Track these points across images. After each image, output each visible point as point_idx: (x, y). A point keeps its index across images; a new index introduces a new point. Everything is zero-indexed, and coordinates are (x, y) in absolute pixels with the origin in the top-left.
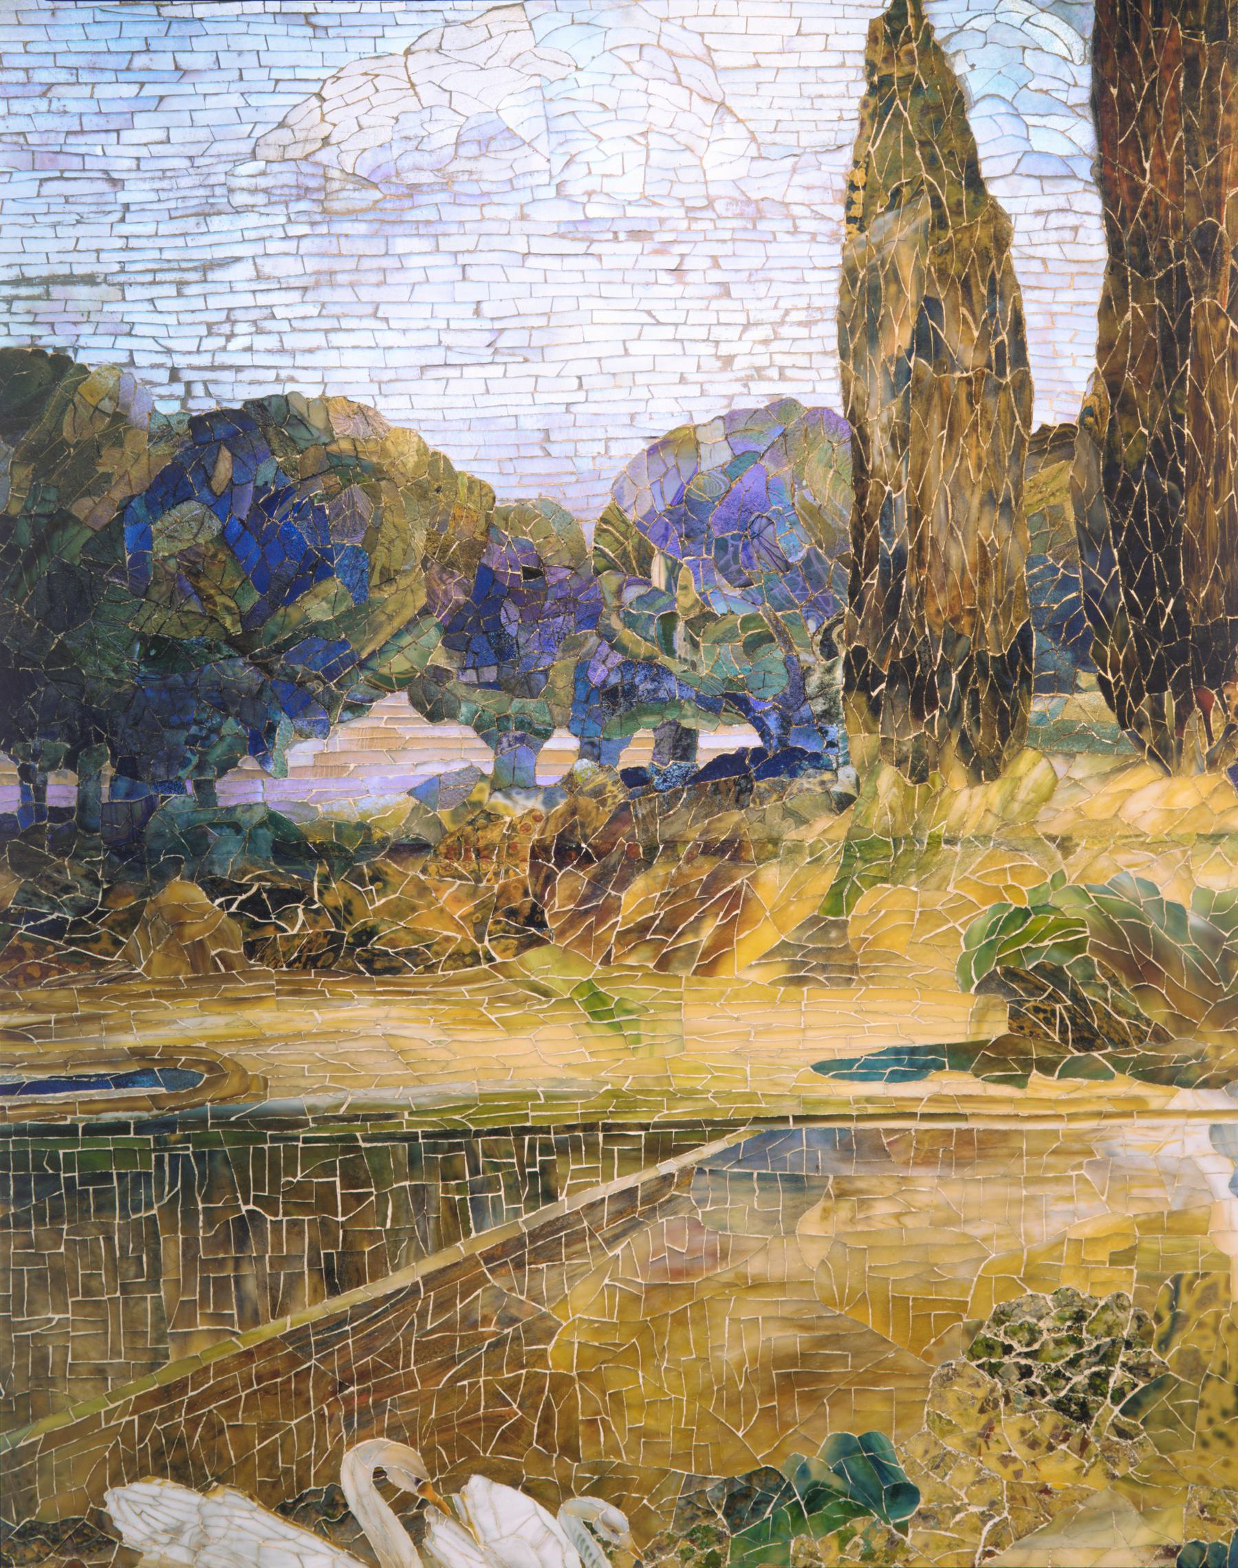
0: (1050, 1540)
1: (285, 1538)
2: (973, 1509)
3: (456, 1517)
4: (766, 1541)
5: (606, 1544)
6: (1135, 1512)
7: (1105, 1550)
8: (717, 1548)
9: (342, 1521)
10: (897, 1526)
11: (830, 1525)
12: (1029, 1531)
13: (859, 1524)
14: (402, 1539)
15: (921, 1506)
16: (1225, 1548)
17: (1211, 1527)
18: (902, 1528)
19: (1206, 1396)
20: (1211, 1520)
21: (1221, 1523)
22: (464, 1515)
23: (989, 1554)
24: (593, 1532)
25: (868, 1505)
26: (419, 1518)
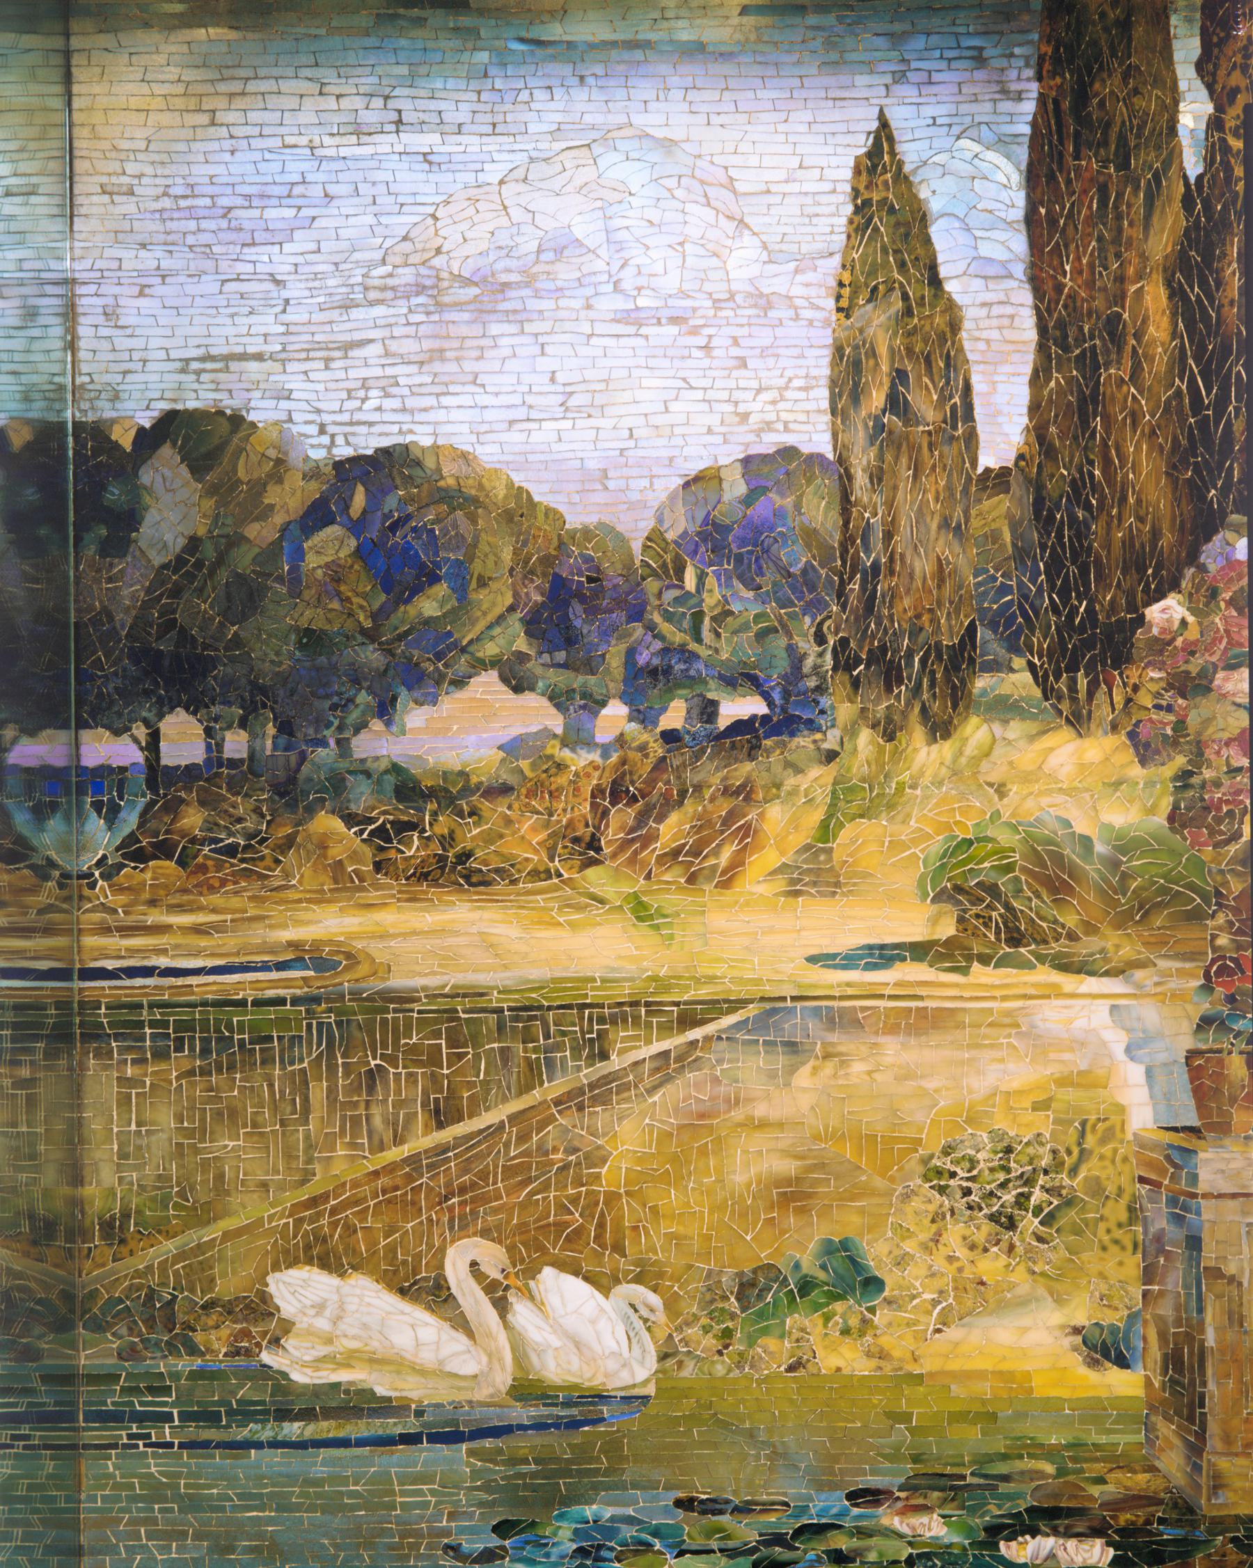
0: (986, 1321)
1: (403, 1313)
2: (928, 1296)
3: (532, 1298)
4: (767, 1319)
5: (646, 1320)
7: (1025, 1330)
8: (730, 1324)
9: (445, 1300)
10: (869, 1309)
11: (816, 1307)
12: (969, 1314)
13: (839, 1307)
14: (491, 1315)
15: (886, 1293)
17: (1108, 1311)
18: (872, 1310)
19: (1106, 1211)
20: (1109, 1306)
22: (538, 1297)
23: (938, 1331)
24: (636, 1311)
26: (504, 1298)
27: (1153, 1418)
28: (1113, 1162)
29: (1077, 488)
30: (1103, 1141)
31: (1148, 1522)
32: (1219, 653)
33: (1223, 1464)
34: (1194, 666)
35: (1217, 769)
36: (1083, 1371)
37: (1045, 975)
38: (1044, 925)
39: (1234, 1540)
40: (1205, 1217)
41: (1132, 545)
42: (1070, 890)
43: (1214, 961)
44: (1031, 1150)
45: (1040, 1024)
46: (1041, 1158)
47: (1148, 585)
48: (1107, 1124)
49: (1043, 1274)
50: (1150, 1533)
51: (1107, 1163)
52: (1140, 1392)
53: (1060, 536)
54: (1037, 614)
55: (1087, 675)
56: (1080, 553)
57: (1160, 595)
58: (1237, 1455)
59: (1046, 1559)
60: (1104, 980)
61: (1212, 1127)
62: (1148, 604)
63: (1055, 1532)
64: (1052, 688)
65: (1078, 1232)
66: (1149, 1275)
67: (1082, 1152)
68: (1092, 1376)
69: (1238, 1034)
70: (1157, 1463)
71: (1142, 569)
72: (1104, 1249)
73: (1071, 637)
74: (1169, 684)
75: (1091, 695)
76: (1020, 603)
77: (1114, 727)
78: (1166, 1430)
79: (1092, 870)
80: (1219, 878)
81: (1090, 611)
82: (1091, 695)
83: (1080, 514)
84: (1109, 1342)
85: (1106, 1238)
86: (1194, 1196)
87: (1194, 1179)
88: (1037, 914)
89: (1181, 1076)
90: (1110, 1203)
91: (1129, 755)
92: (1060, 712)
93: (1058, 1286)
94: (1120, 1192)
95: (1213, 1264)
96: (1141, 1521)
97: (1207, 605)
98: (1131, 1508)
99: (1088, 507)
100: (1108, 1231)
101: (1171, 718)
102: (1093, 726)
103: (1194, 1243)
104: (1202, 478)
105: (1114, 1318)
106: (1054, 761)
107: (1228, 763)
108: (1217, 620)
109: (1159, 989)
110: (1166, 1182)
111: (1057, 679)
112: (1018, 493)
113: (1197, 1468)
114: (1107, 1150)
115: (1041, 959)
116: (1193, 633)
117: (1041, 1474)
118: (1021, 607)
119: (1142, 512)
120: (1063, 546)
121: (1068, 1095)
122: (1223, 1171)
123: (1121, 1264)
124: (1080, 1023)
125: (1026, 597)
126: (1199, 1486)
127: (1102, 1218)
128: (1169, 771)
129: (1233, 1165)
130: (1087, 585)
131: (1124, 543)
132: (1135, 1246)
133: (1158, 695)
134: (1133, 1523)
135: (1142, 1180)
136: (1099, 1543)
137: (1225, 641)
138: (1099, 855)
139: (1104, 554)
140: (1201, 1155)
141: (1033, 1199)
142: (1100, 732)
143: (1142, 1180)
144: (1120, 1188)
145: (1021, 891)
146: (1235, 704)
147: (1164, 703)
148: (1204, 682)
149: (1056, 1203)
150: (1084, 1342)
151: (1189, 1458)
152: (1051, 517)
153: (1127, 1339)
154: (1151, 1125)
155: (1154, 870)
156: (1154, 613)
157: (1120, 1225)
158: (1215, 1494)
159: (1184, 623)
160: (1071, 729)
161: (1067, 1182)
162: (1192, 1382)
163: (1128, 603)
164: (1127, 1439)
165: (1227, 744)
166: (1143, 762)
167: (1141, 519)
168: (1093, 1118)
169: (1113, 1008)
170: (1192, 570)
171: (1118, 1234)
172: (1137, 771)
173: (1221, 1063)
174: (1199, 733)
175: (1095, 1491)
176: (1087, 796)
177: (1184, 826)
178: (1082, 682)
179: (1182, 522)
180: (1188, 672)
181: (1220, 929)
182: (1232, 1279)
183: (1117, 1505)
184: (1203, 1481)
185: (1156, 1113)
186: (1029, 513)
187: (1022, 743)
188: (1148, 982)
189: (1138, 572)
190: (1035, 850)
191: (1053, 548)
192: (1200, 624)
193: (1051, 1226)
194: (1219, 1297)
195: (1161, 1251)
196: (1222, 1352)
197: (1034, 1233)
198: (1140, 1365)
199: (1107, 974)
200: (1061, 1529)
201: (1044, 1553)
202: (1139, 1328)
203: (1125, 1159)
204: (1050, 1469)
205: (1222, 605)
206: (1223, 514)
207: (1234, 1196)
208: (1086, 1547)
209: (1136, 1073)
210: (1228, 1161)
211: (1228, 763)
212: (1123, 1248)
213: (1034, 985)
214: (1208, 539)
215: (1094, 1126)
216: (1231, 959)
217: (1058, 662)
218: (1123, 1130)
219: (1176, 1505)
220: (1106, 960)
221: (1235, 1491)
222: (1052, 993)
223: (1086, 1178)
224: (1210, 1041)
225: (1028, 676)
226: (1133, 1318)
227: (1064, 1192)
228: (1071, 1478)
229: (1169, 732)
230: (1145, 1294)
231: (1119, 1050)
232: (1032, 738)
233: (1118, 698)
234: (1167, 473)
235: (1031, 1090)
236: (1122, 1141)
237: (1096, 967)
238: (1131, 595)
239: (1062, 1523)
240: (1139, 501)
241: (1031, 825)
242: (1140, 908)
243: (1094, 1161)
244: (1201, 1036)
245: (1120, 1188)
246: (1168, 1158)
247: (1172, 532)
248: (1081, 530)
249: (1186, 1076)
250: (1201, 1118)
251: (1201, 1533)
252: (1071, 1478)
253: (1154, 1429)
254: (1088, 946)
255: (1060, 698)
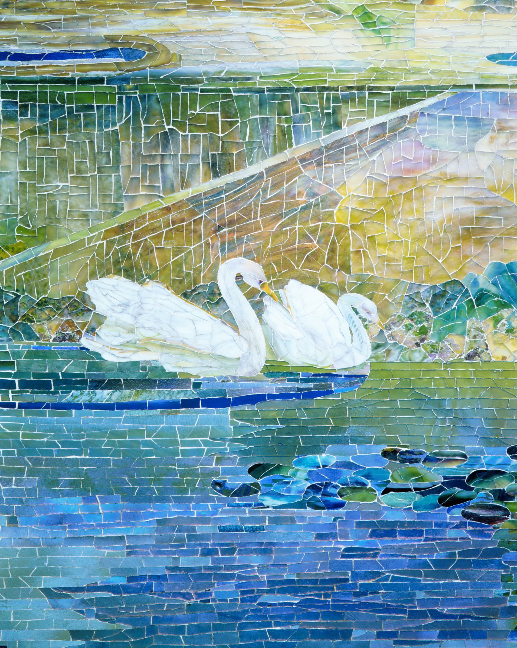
3: (281, 302)
4: (453, 320)
5: (364, 320)
8: (426, 324)
9: (217, 303)
14: (251, 313)
22: (285, 302)
24: (357, 313)
25: (511, 302)
26: (261, 302)
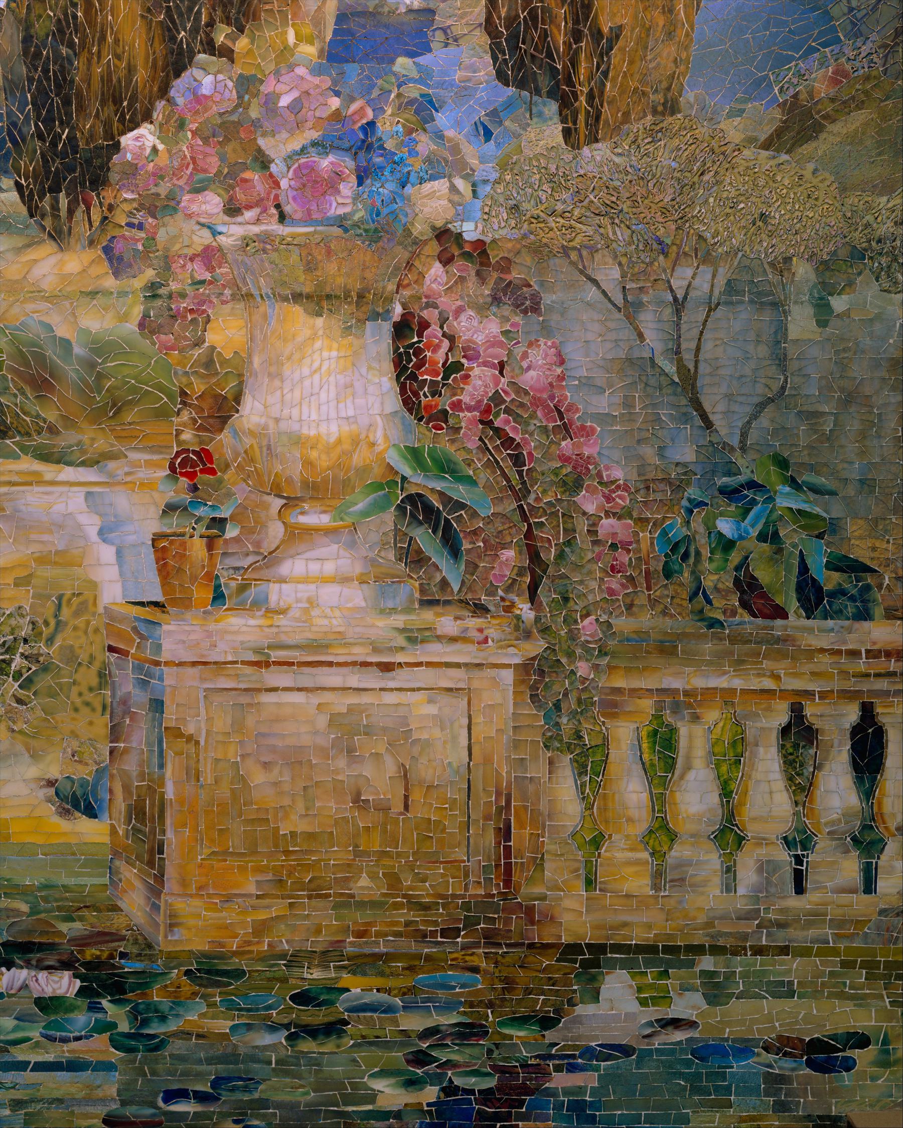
6: (27, 755)
16: (88, 781)
17: (80, 767)
19: (78, 677)
20: (80, 762)
21: (87, 764)
27: (117, 863)
28: (86, 632)
29: (61, 31)
30: (77, 614)
31: (111, 956)
32: (186, 177)
33: (180, 905)
34: (163, 189)
35: (182, 281)
36: (56, 820)
37: (27, 464)
38: (28, 419)
39: (188, 973)
40: (166, 683)
41: (110, 80)
42: (50, 387)
43: (178, 454)
44: (13, 622)
45: (23, 508)
46: (20, 628)
47: (123, 116)
48: (81, 599)
49: (21, 732)
50: (114, 966)
51: (80, 633)
52: (107, 839)
53: (46, 71)
54: (24, 140)
55: (68, 195)
56: (63, 83)
57: (134, 125)
58: (191, 896)
59: (20, 989)
60: (80, 469)
61: (174, 602)
62: (123, 133)
63: (28, 965)
64: (37, 207)
65: (53, 694)
66: (115, 733)
67: (58, 623)
68: (64, 825)
69: (199, 520)
70: (119, 903)
71: (117, 101)
72: (76, 710)
73: (54, 161)
74: (141, 204)
75: (71, 212)
76: (9, 128)
77: (91, 243)
78: (129, 873)
79: (71, 371)
80: (184, 380)
81: (71, 139)
82: (71, 212)
83: (64, 51)
84: (79, 793)
85: (78, 701)
86: (157, 663)
87: (158, 648)
88: (22, 409)
89: (148, 556)
90: (82, 670)
91: (104, 267)
92: (43, 228)
93: (34, 743)
94: (91, 661)
95: (173, 724)
96: (105, 955)
97: (175, 135)
98: (96, 943)
99: (71, 45)
100: (80, 694)
101: (142, 235)
102: (72, 241)
103: (157, 705)
104: (173, 22)
105: (85, 772)
106: (38, 271)
107: (192, 277)
108: (184, 148)
109: (128, 479)
110: (133, 651)
111: (41, 198)
112: (9, 32)
113: (156, 908)
114: (80, 622)
115: (24, 449)
116: (163, 160)
117: (17, 912)
118: (10, 133)
119: (119, 51)
120: (48, 79)
121: (47, 572)
122: (184, 642)
123: (91, 723)
124: (59, 508)
125: (15, 125)
126: (157, 925)
127: (74, 683)
128: (138, 283)
129: (193, 637)
130: (69, 115)
131: (102, 77)
132: (104, 708)
133: (130, 214)
134: (98, 957)
135: (111, 649)
136: (67, 974)
137: (191, 166)
138: (77, 357)
139: (84, 87)
140: (165, 627)
141: (13, 665)
142: (79, 246)
143: (111, 649)
144: (91, 656)
145: (7, 388)
146: (199, 223)
147: (136, 222)
148: (172, 203)
149: (34, 668)
150: (57, 794)
151: (149, 899)
152: (38, 55)
153: (95, 793)
154: (120, 599)
155: (126, 371)
156: (127, 140)
157: (91, 689)
158: (171, 931)
159: (155, 149)
160: (53, 243)
161: (44, 650)
162: (153, 831)
163: (105, 132)
164: (91, 880)
165: (192, 259)
166: (116, 274)
167: (118, 57)
168: (69, 593)
169: (88, 495)
170: (163, 102)
171: (89, 697)
172: (110, 282)
173: (184, 544)
174: (166, 249)
175: (64, 927)
176: (67, 303)
177: (152, 332)
178: (64, 201)
179: (155, 60)
180: (158, 195)
181: (184, 425)
182: (190, 738)
183: (83, 942)
184: (161, 919)
185: (124, 589)
186: (19, 48)
187: (10, 256)
188: (119, 472)
189: (115, 103)
190: (21, 351)
191: (40, 81)
192: (169, 151)
193: (29, 689)
194: (178, 754)
195: (127, 712)
196: (181, 801)
197: (14, 695)
198: (107, 814)
199: (83, 464)
200: (34, 962)
201: (18, 984)
202: (106, 782)
203: (97, 631)
204: (24, 908)
205: (189, 134)
206: (192, 55)
207: (194, 664)
208: (56, 979)
209: (108, 553)
210: (189, 633)
211: (192, 277)
212: (93, 710)
213: (18, 473)
214: (178, 75)
215: (69, 600)
216: (194, 452)
217: (42, 183)
218: (95, 604)
219: (136, 942)
220: (83, 452)
221: (189, 929)
222: (35, 480)
223: (61, 647)
224: (174, 524)
225: (14, 196)
226: (100, 773)
227: (41, 659)
228: (43, 916)
229: (140, 247)
230: (111, 752)
231: (92, 533)
232: (18, 251)
233: (96, 217)
234: (142, 16)
235: (13, 568)
236: (94, 614)
237: (73, 458)
238: (108, 124)
239: (35, 957)
240: (117, 41)
241: (18, 329)
242: (114, 405)
243: (69, 630)
244: (166, 521)
245: (91, 656)
246: (135, 629)
247: (145, 69)
248: (64, 66)
249: (152, 556)
250: (165, 594)
251: (159, 965)
252: (43, 916)
253: (118, 873)
254: (67, 439)
255: (43, 216)
